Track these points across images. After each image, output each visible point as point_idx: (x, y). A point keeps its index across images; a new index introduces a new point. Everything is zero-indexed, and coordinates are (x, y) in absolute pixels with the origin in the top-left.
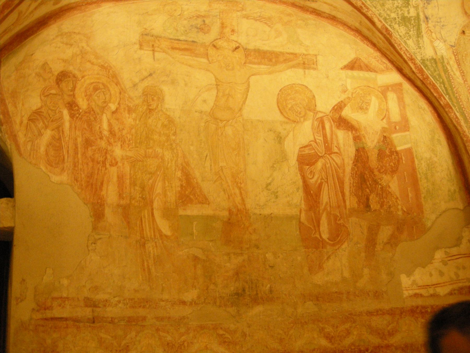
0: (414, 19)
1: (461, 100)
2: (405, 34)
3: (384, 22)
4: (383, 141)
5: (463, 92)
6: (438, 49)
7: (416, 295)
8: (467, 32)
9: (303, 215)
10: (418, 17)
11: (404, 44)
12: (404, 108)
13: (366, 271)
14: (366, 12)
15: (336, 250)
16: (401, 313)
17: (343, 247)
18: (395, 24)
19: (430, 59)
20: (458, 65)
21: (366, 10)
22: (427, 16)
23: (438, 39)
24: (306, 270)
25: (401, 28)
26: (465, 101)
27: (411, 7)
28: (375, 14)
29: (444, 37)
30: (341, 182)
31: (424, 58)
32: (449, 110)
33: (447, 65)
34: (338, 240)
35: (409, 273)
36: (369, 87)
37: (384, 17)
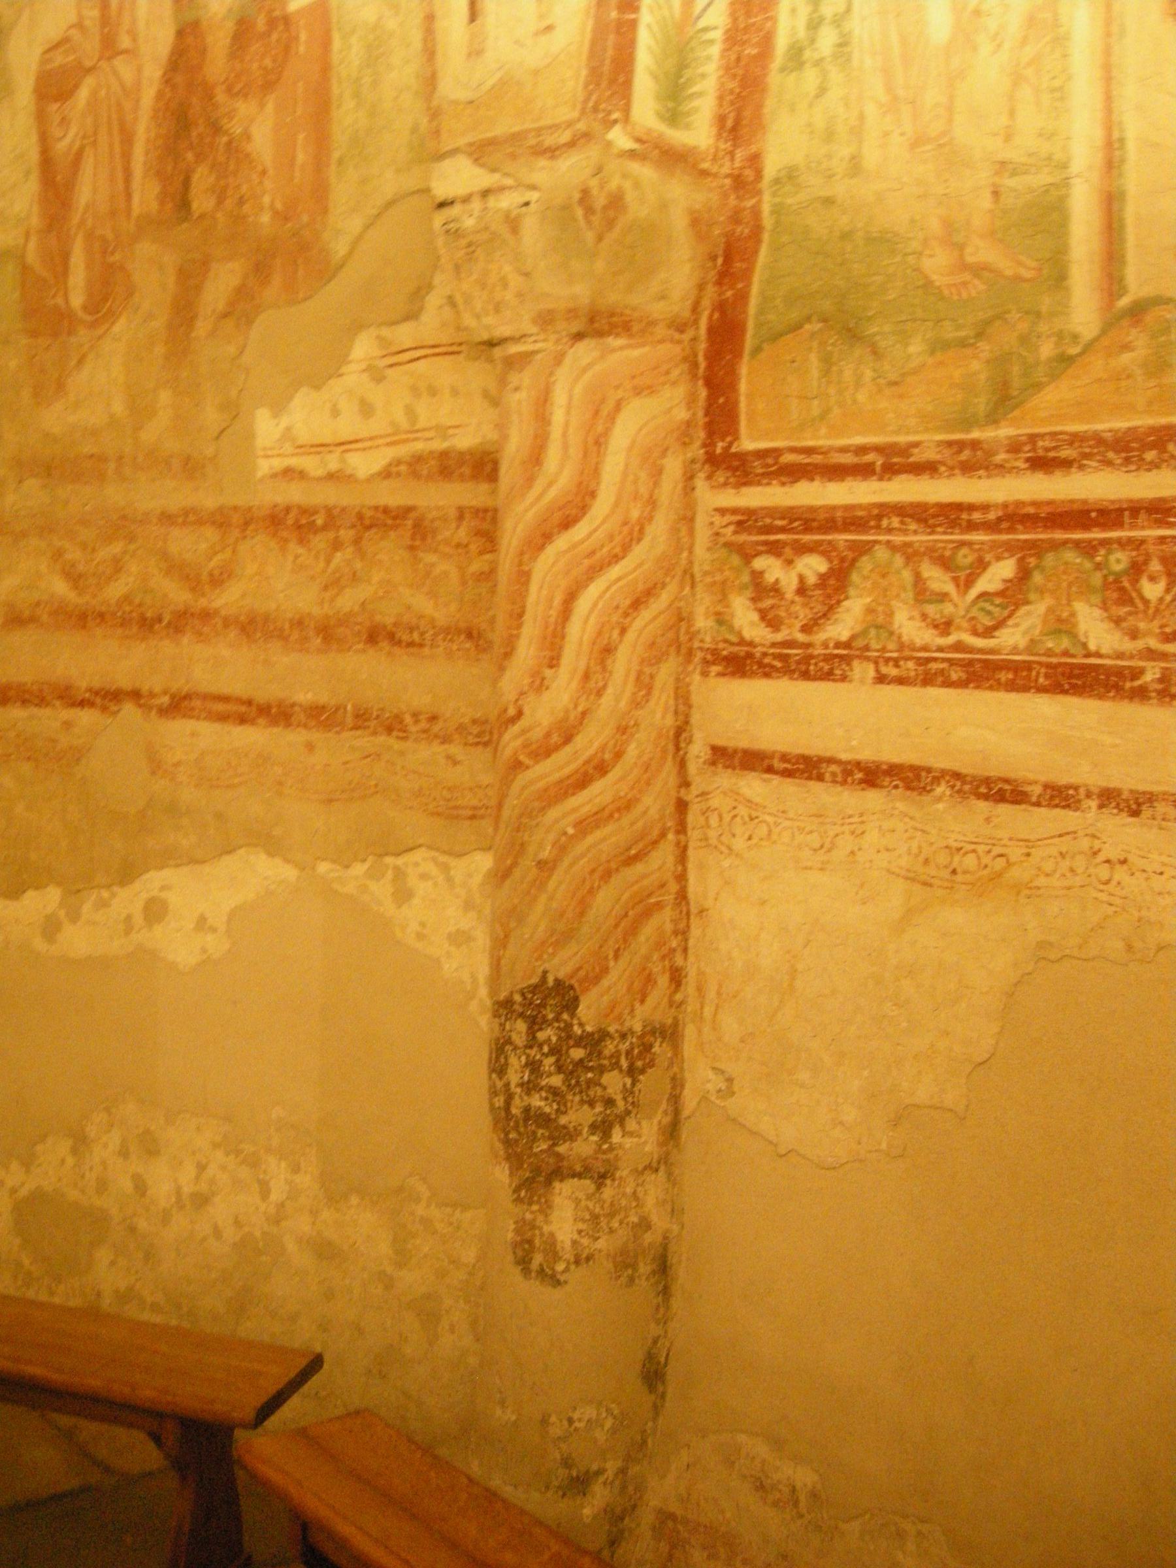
7: (288, 473)
9: (32, 245)
13: (165, 397)
15: (100, 338)
16: (247, 524)
17: (117, 328)
24: (26, 394)
30: (128, 139)
34: (105, 310)
35: (278, 408)
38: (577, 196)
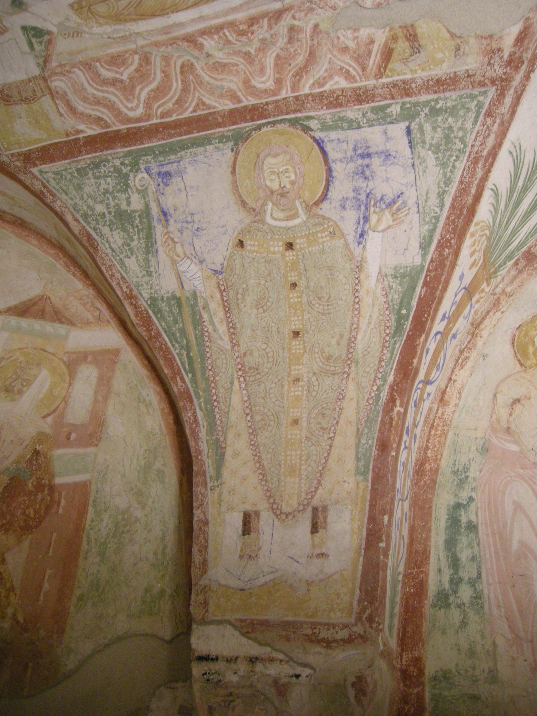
0: (139, 216)
1: (216, 385)
2: (123, 245)
3: (82, 222)
4: (30, 460)
5: (226, 368)
6: (186, 276)
8: (249, 242)
10: (147, 212)
11: (118, 266)
12: (106, 399)
14: (52, 202)
18: (104, 226)
19: (168, 298)
20: (226, 312)
21: (51, 197)
22: (165, 210)
23: (188, 258)
25: (114, 233)
26: (225, 386)
27: (132, 192)
28: (66, 207)
29: (200, 255)
31: (156, 295)
32: (184, 405)
33: (202, 311)
36: (45, 351)
37: (82, 212)
38: (351, 679)
